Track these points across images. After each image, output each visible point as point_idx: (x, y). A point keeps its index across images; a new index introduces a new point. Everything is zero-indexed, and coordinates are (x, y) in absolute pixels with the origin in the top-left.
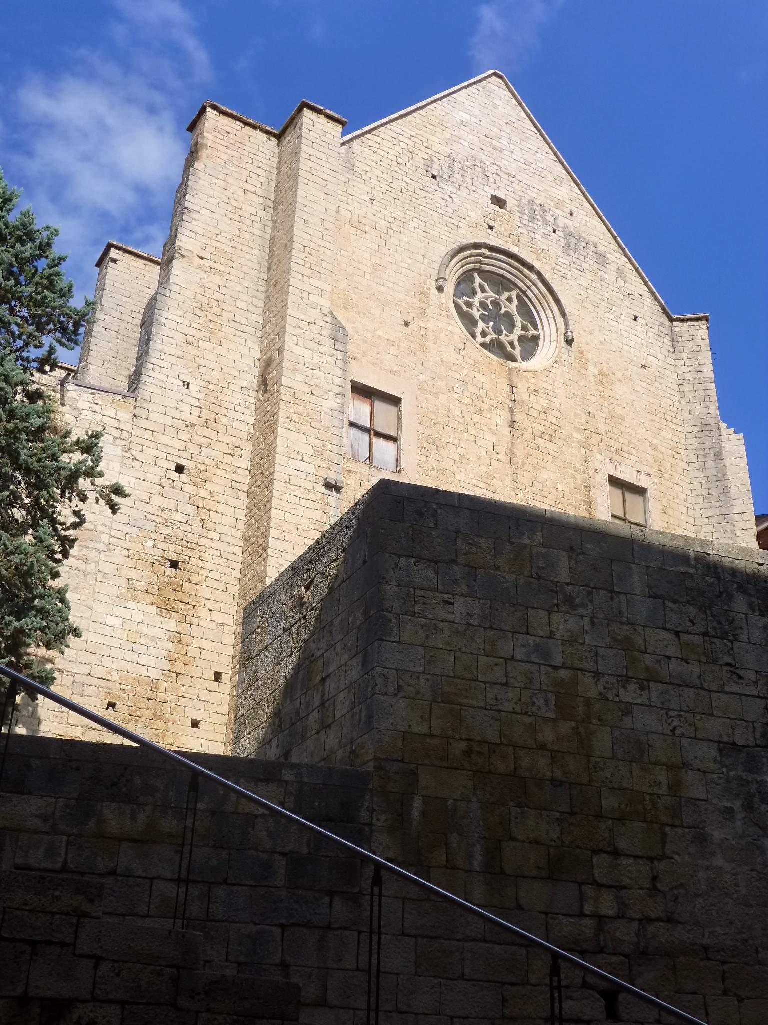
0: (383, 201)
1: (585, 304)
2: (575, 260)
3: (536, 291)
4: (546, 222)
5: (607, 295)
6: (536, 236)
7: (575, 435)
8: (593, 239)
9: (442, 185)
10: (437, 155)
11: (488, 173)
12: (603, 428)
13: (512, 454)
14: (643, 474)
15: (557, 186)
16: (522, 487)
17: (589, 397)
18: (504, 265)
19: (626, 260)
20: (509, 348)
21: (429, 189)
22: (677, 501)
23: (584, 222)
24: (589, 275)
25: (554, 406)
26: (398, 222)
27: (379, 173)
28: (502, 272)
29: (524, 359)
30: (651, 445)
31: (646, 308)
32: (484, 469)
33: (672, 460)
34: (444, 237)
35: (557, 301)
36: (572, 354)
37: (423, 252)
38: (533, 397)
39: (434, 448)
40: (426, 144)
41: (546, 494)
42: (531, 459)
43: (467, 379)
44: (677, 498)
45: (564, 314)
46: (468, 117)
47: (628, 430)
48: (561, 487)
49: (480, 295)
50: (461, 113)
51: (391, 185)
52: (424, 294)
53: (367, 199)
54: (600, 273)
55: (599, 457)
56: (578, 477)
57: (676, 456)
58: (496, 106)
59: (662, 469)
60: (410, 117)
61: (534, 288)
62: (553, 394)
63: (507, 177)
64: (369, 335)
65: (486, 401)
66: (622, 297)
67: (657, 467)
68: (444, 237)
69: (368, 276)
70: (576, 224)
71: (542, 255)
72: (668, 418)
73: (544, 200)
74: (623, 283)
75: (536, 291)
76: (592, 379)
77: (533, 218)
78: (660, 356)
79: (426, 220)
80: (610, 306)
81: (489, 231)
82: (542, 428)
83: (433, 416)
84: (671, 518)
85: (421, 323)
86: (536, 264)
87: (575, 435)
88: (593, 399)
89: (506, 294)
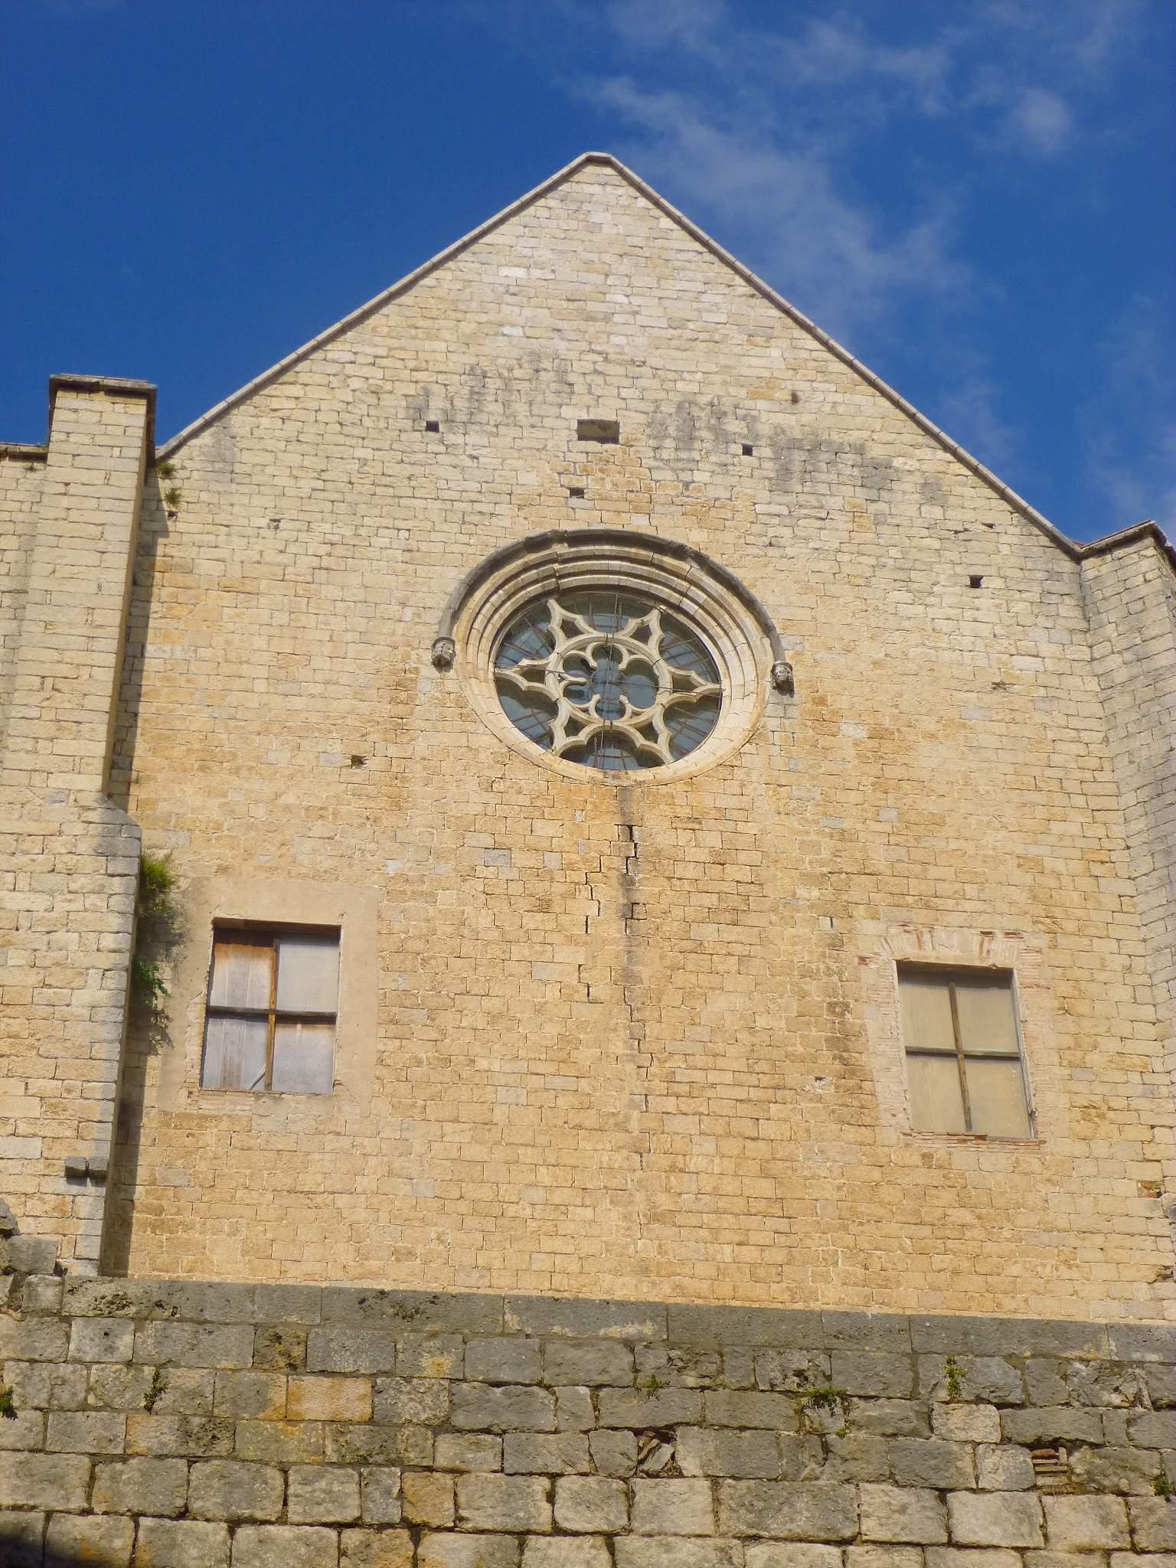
0: (302, 516)
1: (832, 589)
2: (802, 498)
3: (699, 596)
4: (722, 438)
5: (893, 552)
6: (698, 476)
7: (801, 892)
8: (855, 436)
9: (451, 439)
10: (441, 378)
11: (571, 378)
12: (879, 858)
13: (628, 977)
14: (1000, 935)
15: (758, 351)
16: (655, 1047)
17: (841, 796)
18: (616, 564)
19: (949, 457)
20: (640, 741)
21: (420, 457)
22: (1101, 976)
23: (827, 408)
24: (842, 522)
25: (742, 841)
26: (339, 550)
27: (294, 459)
28: (614, 579)
29: (679, 751)
30: (1022, 861)
31: (1005, 550)
32: (552, 1030)
33: (1086, 884)
34: (457, 548)
35: (750, 603)
36: (794, 712)
37: (399, 594)
38: (684, 837)
39: (420, 1015)
40: (411, 364)
41: (720, 1047)
42: (679, 978)
43: (508, 841)
44: (1103, 968)
45: (767, 629)
46: (520, 273)
47: (953, 845)
48: (761, 1022)
49: (564, 645)
50: (504, 271)
51: (325, 476)
52: (402, 685)
53: (264, 522)
54: (873, 508)
55: (869, 927)
56: (812, 987)
57: (1097, 869)
58: (594, 228)
59: (1058, 912)
60: (373, 321)
61: (694, 592)
62: (737, 815)
63: (621, 370)
64: (260, 812)
65: (559, 876)
66: (937, 544)
67: (1040, 911)
68: (457, 548)
69: (260, 686)
70: (806, 418)
71: (713, 513)
72: (1070, 786)
73: (718, 390)
74: (937, 513)
75: (702, 597)
76: (850, 752)
77: (688, 438)
78: (1046, 649)
79: (410, 524)
80: (902, 575)
81: (575, 501)
82: (710, 900)
83: (419, 945)
84: (1085, 1022)
85: (393, 751)
86: (694, 538)
87: (801, 892)
88: (853, 797)
89: (633, 624)
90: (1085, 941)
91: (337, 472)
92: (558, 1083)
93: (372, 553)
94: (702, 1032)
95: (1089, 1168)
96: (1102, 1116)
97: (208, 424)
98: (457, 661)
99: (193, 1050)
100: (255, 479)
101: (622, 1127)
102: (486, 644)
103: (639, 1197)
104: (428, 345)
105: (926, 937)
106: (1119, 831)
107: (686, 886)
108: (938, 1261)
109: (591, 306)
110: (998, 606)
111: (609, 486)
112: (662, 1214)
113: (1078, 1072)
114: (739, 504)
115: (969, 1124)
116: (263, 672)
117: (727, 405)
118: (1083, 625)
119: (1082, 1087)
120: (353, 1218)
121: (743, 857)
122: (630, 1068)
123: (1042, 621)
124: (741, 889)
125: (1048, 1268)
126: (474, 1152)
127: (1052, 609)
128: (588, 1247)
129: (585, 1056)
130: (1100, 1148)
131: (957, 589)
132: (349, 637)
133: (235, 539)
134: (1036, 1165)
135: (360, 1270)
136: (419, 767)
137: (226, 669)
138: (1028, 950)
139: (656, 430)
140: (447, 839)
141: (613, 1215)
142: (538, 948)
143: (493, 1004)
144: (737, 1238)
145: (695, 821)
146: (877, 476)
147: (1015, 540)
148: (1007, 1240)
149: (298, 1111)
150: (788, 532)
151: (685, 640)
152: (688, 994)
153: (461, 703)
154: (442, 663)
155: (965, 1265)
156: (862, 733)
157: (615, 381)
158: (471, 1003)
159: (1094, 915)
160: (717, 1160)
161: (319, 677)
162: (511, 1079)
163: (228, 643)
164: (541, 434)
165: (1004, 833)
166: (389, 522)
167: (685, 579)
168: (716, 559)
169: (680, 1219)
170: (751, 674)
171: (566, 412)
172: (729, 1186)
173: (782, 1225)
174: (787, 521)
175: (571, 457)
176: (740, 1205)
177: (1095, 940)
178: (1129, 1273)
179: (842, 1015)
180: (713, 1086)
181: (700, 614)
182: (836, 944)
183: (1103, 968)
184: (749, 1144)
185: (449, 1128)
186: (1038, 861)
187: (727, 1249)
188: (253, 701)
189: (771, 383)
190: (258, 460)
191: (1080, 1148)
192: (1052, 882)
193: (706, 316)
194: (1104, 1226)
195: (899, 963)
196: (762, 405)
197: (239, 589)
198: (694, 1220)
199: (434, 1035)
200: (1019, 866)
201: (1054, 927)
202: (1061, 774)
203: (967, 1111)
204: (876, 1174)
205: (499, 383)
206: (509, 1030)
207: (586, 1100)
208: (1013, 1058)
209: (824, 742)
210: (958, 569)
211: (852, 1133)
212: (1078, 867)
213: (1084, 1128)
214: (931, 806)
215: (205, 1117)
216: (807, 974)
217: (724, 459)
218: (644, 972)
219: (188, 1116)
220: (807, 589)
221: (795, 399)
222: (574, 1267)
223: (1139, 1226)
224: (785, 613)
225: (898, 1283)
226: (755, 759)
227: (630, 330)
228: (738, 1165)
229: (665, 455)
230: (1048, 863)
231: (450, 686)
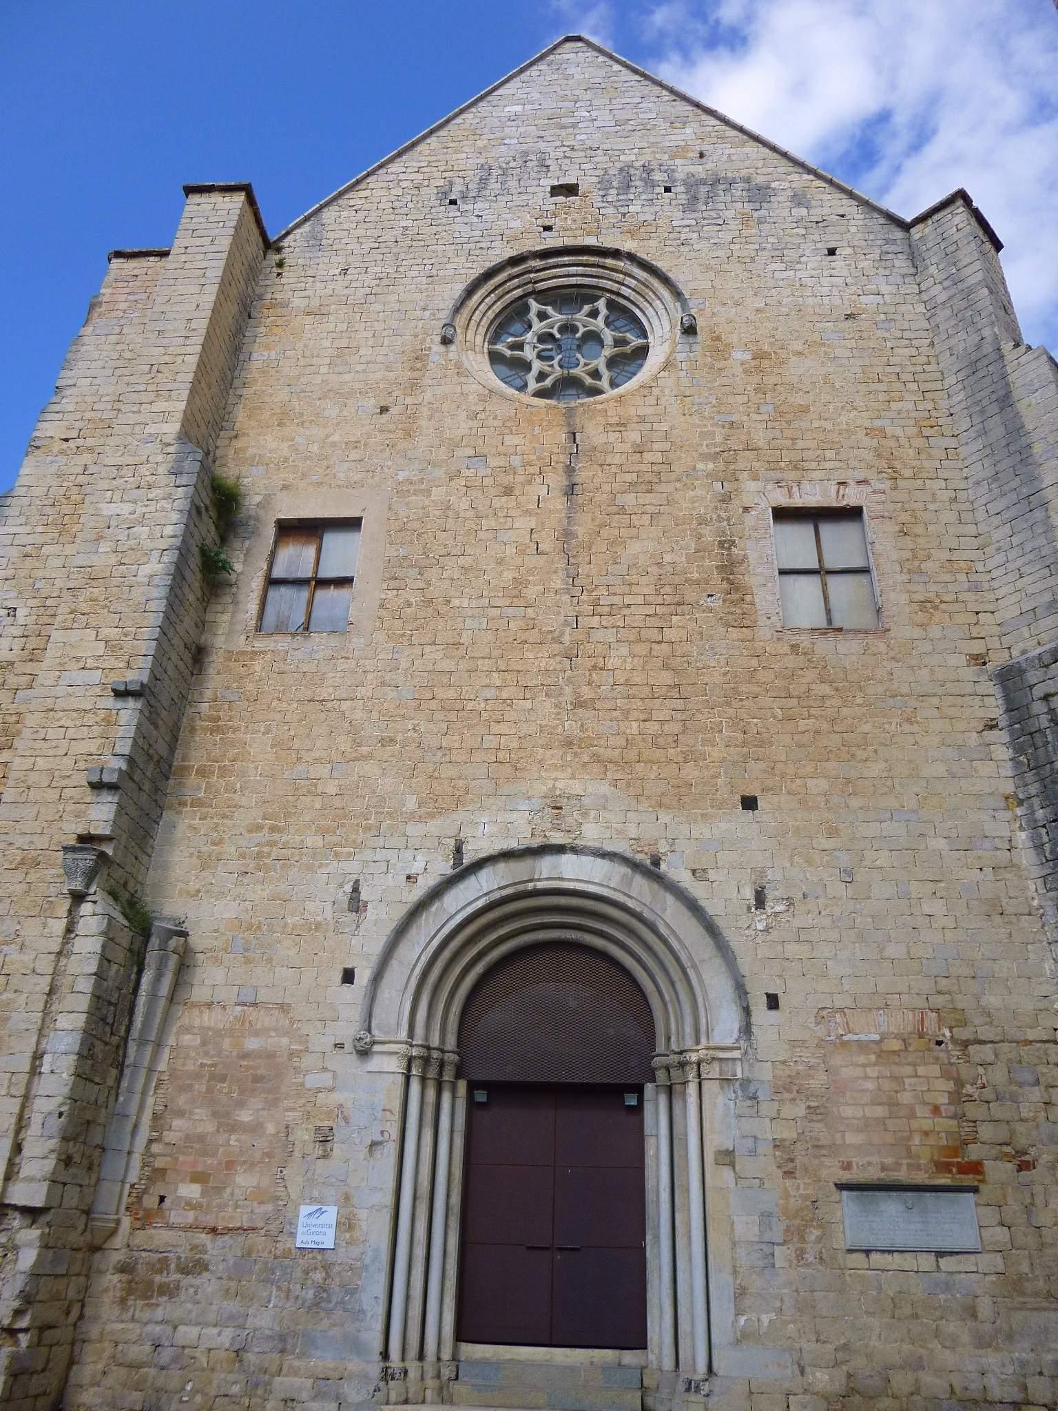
3: (630, 282)
4: (650, 183)
5: (771, 240)
7: (700, 466)
8: (744, 173)
9: (464, 207)
11: (548, 163)
12: (760, 438)
13: (568, 534)
14: (852, 483)
16: (585, 582)
17: (731, 400)
18: (573, 270)
19: (811, 177)
21: (444, 221)
22: (932, 507)
23: (725, 158)
24: (734, 225)
26: (385, 282)
27: (361, 232)
28: (573, 280)
29: (613, 384)
30: (869, 432)
31: (853, 229)
32: (508, 575)
33: (920, 442)
34: (462, 271)
35: (665, 280)
36: (697, 347)
38: (613, 437)
39: (413, 572)
40: (442, 169)
41: (635, 579)
42: (605, 533)
43: (485, 451)
44: (934, 500)
45: (678, 295)
46: (518, 108)
47: (816, 424)
48: (667, 558)
50: (507, 109)
52: (419, 358)
54: (756, 214)
55: (753, 486)
58: (568, 77)
59: (897, 464)
60: (420, 148)
61: (629, 281)
62: (652, 419)
63: (583, 154)
64: (315, 448)
65: (520, 471)
69: (324, 370)
70: (709, 166)
72: (904, 377)
73: (648, 157)
74: (804, 212)
75: (633, 283)
76: (739, 370)
78: (884, 289)
79: (433, 261)
80: (778, 253)
83: (416, 525)
84: (921, 540)
85: (409, 400)
86: (628, 246)
87: (700, 466)
88: (740, 399)
90: (919, 482)
91: (388, 236)
92: (510, 612)
93: (405, 281)
94: (622, 569)
95: (927, 647)
96: (936, 608)
97: (306, 219)
98: (459, 337)
99: (253, 607)
100: (334, 247)
101: (557, 640)
102: (482, 330)
103: (568, 690)
104: (455, 157)
105: (795, 489)
106: (943, 404)
107: (614, 469)
108: (803, 725)
109: (564, 120)
110: (849, 265)
111: (569, 222)
112: (585, 702)
113: (916, 577)
114: (660, 222)
115: (830, 621)
116: (327, 361)
117: (655, 165)
118: (913, 271)
119: (920, 588)
120: (354, 717)
121: (656, 446)
122: (566, 598)
123: (881, 271)
124: (655, 468)
125: (893, 727)
126: (448, 665)
127: (889, 264)
128: (525, 729)
129: (532, 592)
130: (935, 632)
131: (819, 258)
132: (386, 333)
133: (318, 284)
134: (882, 647)
135: (354, 755)
136: (426, 409)
137: (302, 361)
138: (874, 492)
139: (604, 184)
140: (442, 454)
141: (548, 705)
142: (501, 520)
143: (466, 561)
144: (643, 717)
145: (622, 425)
146: (760, 194)
147: (861, 223)
148: (859, 705)
149: (320, 642)
150: (695, 235)
151: (621, 313)
152: (611, 544)
153: (459, 365)
154: (446, 341)
155: (825, 726)
156: (747, 356)
157: (578, 161)
158: (449, 561)
159: (926, 464)
160: (629, 660)
161: (363, 360)
162: (476, 612)
163: (305, 346)
164: (523, 197)
165: (855, 412)
166: (420, 261)
167: (621, 272)
168: (642, 255)
169: (598, 705)
170: (667, 327)
171: (543, 182)
172: (638, 678)
173: (679, 704)
174: (695, 229)
175: (544, 208)
176: (646, 691)
177: (927, 481)
178: (961, 726)
179: (730, 549)
180: (628, 606)
181: (633, 296)
182: (726, 499)
183: (934, 500)
184: (655, 646)
185: (427, 649)
186: (882, 430)
187: (635, 725)
188: (318, 379)
189: (686, 148)
190: (337, 236)
191: (918, 633)
192: (892, 444)
193: (641, 116)
194: (940, 691)
195: (774, 509)
196: (679, 162)
197: (319, 313)
198: (609, 705)
199: (422, 585)
200: (867, 434)
201: (895, 475)
202: (898, 370)
203: (828, 611)
204: (754, 662)
205: (500, 172)
206: (476, 578)
207: (531, 622)
208: (865, 571)
209: (719, 365)
210: (819, 245)
211: (735, 633)
212: (912, 431)
213: (921, 617)
214: (799, 399)
215: (255, 653)
216: (703, 522)
217: (650, 196)
218: (580, 531)
219: (244, 653)
220: (708, 268)
221: (702, 155)
222: (515, 745)
223: (969, 688)
224: (692, 285)
225: (771, 744)
226: (668, 380)
227: (588, 130)
228: (645, 662)
229: (610, 199)
230: (889, 431)
231: (451, 356)
